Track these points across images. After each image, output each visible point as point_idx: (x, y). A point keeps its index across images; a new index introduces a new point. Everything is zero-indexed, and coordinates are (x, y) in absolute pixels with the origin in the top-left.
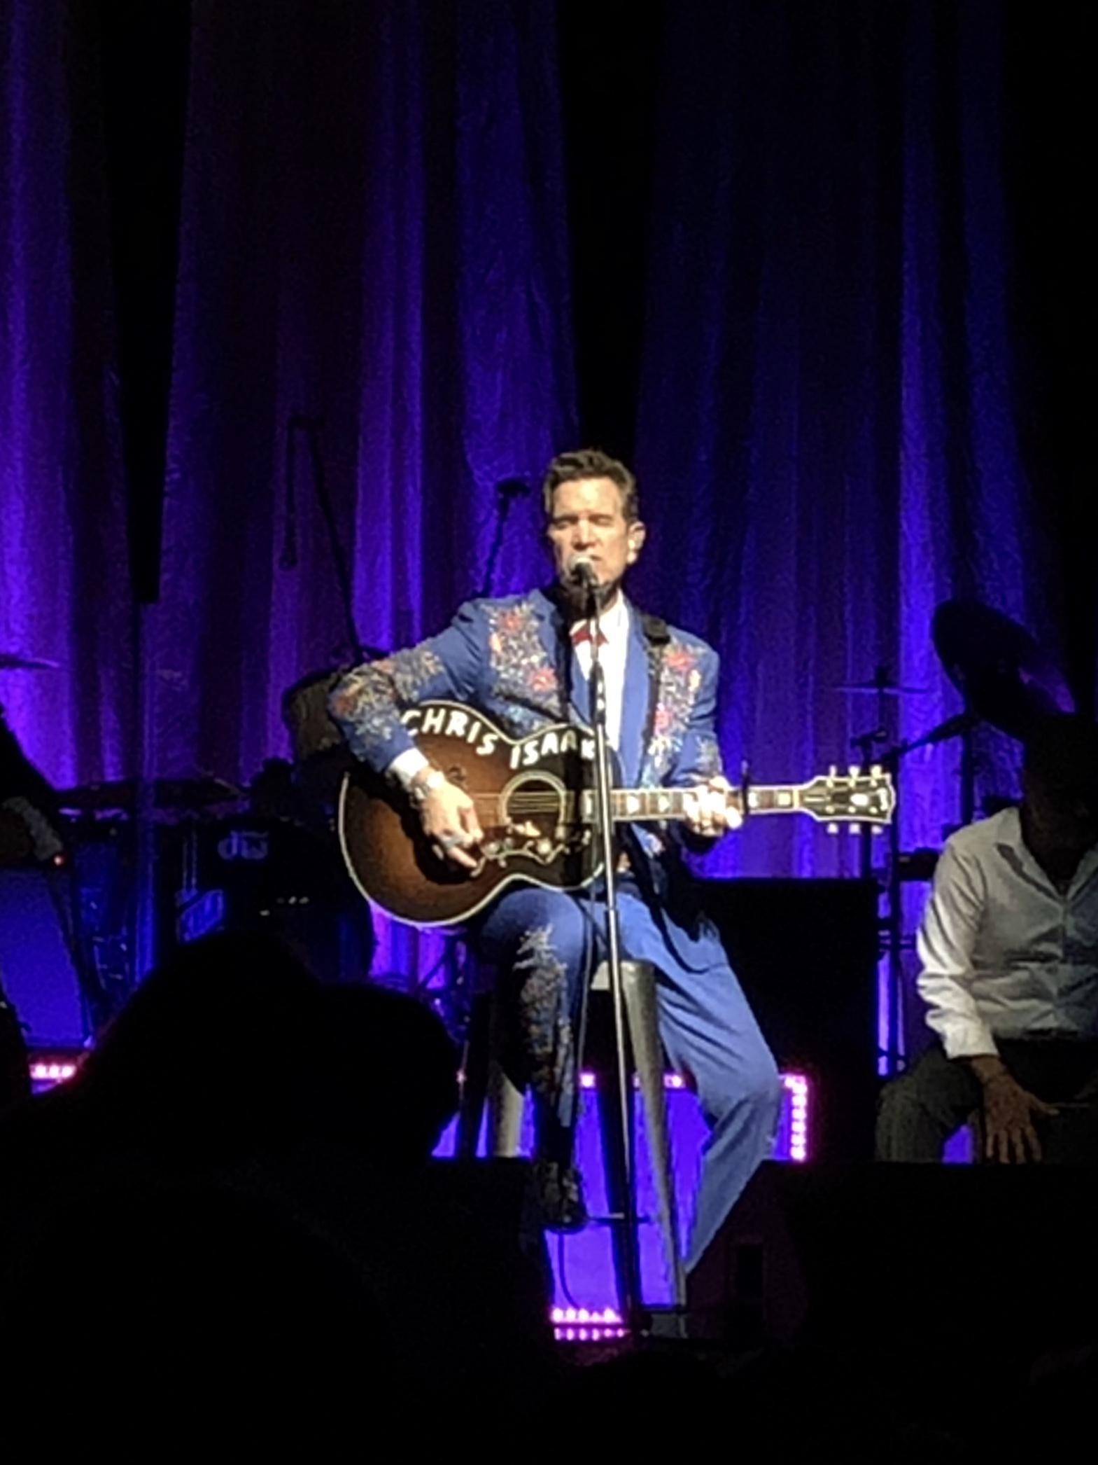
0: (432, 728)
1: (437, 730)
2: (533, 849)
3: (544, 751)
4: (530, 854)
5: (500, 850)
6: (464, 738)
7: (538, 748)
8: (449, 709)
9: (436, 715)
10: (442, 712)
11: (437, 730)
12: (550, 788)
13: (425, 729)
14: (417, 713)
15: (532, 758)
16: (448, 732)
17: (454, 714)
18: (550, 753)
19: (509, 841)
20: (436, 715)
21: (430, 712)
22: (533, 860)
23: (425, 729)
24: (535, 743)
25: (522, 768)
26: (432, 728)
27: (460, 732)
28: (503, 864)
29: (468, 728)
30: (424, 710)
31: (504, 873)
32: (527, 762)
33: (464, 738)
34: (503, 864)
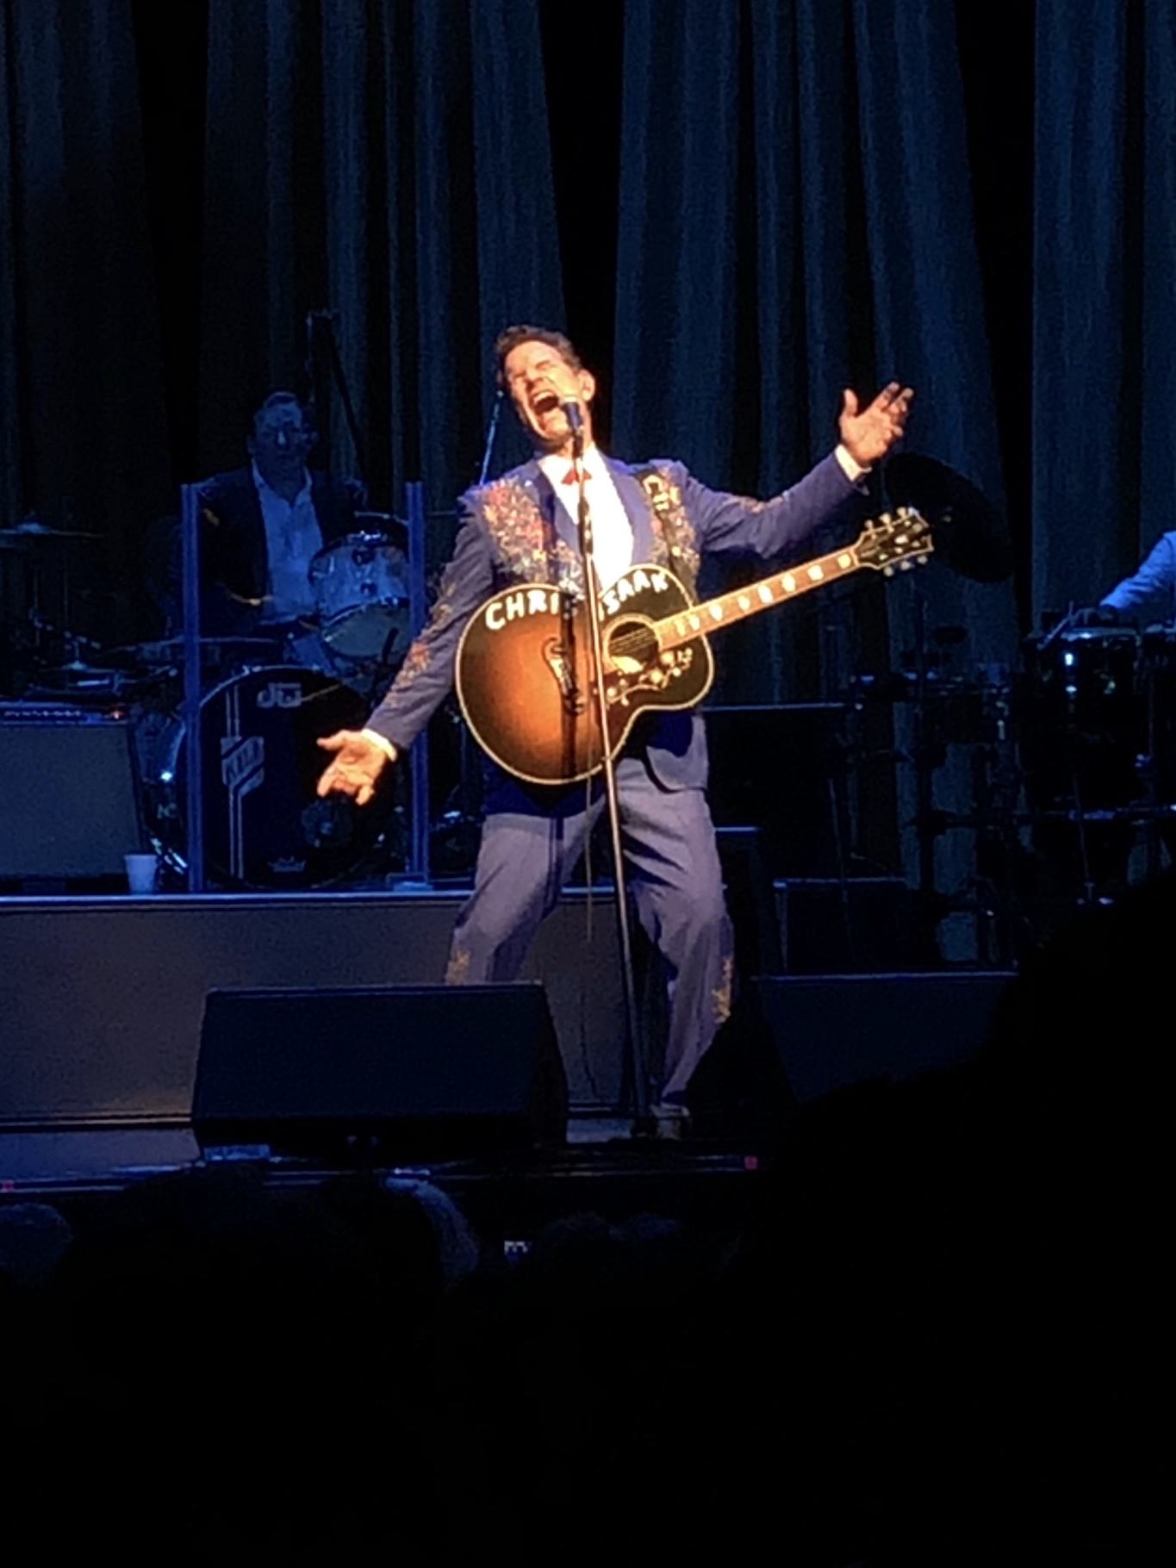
0: (516, 613)
1: (521, 613)
2: (648, 681)
3: (623, 598)
4: (646, 687)
5: (619, 693)
6: (548, 611)
7: (617, 597)
8: (525, 592)
9: (515, 601)
10: (520, 596)
11: (521, 613)
12: (642, 626)
13: (511, 616)
14: (498, 606)
15: (614, 607)
16: (532, 611)
17: (530, 595)
18: (629, 598)
19: (623, 682)
20: (515, 601)
21: (509, 600)
22: (650, 691)
23: (511, 616)
24: (613, 593)
25: (609, 618)
26: (516, 613)
27: (543, 608)
28: (625, 702)
29: (548, 601)
30: (503, 600)
31: (632, 709)
32: (611, 611)
33: (548, 611)
34: (625, 702)
